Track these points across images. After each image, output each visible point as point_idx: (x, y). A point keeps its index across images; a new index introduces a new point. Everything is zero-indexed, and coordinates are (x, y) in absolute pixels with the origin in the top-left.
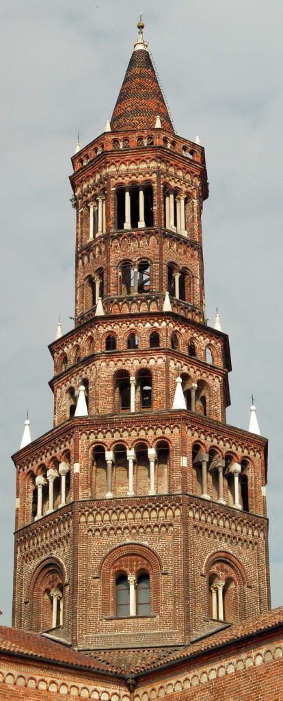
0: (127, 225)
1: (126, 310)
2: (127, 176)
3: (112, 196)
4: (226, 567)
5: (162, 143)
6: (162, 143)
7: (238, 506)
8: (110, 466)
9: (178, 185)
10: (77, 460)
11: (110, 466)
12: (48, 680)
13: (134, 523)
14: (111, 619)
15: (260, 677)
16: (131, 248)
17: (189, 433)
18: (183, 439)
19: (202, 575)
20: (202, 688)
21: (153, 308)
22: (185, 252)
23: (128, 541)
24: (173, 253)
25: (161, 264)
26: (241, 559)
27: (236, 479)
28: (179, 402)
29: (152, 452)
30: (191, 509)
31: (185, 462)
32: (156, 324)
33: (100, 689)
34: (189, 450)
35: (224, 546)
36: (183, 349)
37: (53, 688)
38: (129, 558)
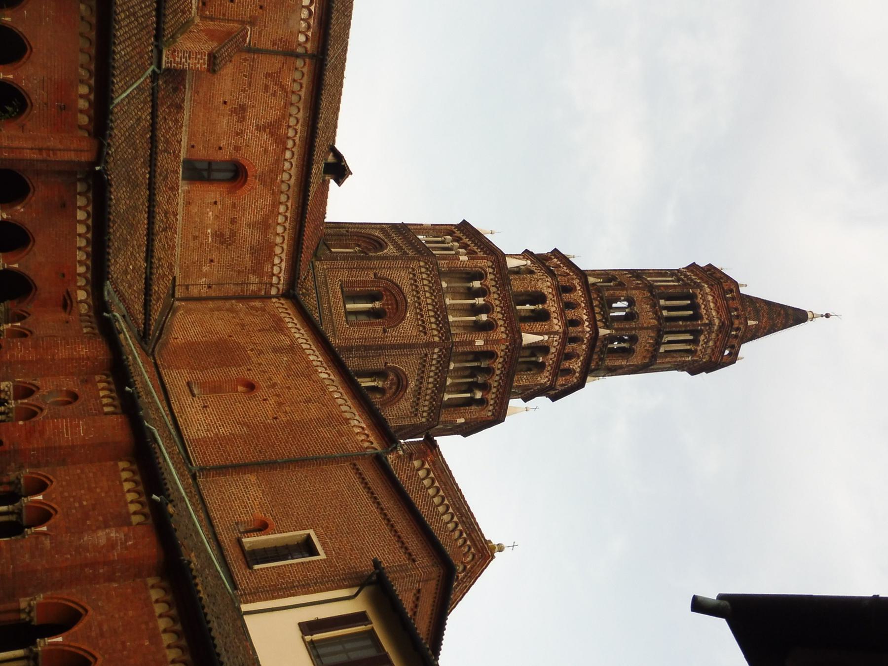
0: (662, 302)
1: (595, 303)
2: (704, 300)
3: (685, 290)
4: (394, 387)
5: (735, 326)
6: (735, 326)
7: (447, 397)
8: (468, 285)
9: (701, 343)
10: (470, 259)
11: (468, 285)
12: (288, 214)
13: (423, 304)
14: (342, 288)
15: (309, 377)
16: (644, 306)
17: (503, 347)
18: (498, 342)
19: (386, 363)
20: (293, 340)
21: (599, 324)
22: (647, 350)
23: (409, 300)
24: (645, 339)
25: (635, 329)
26: (402, 401)
27: (468, 395)
28: (528, 338)
29: (484, 317)
30: (441, 350)
31: (479, 343)
33: (283, 265)
34: (489, 348)
35: (412, 384)
37: (281, 219)
38: (394, 302)
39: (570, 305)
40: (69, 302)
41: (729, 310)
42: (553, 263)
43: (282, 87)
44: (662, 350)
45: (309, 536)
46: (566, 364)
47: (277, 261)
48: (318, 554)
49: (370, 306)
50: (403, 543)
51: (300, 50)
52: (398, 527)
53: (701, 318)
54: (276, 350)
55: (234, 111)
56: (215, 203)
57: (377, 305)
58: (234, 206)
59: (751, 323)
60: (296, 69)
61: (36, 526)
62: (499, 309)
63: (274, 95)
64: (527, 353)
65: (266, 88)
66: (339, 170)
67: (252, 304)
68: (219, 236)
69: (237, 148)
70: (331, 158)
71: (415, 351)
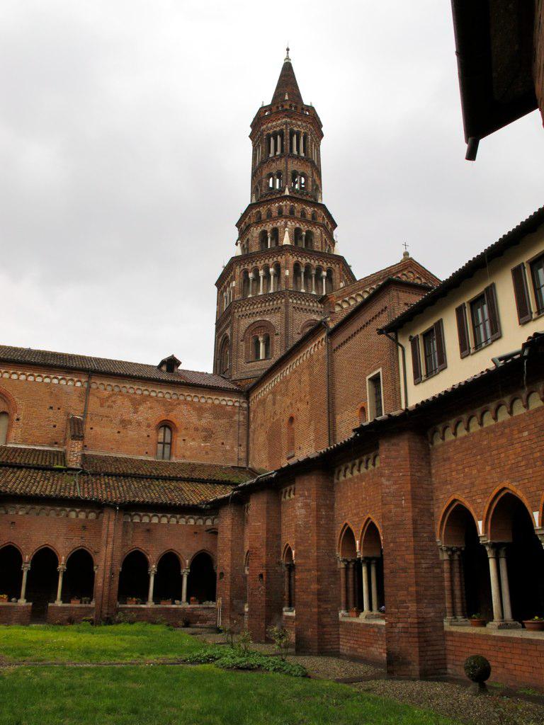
0: (271, 155)
5: (288, 107)
6: (288, 107)
8: (251, 281)
9: (299, 129)
15: (288, 381)
17: (291, 257)
23: (259, 319)
27: (324, 280)
29: (272, 270)
31: (287, 273)
32: (281, 203)
33: (227, 399)
36: (298, 215)
37: (196, 400)
39: (269, 215)
40: (213, 530)
41: (278, 112)
42: (244, 225)
43: (110, 397)
44: (303, 155)
45: (369, 379)
46: (309, 217)
47: (224, 403)
48: (418, 379)
49: (261, 344)
50: (376, 316)
51: (86, 385)
52: (368, 319)
53: (282, 130)
54: (274, 404)
55: (124, 427)
56: (184, 440)
57: (261, 339)
58: (186, 429)
59: (287, 98)
60: (98, 388)
61: (292, 556)
62: (267, 261)
63: (114, 402)
64: (299, 242)
65: (111, 407)
66: (171, 363)
67: (251, 419)
68: (206, 439)
69: (149, 426)
70: (164, 368)
71: (290, 315)
